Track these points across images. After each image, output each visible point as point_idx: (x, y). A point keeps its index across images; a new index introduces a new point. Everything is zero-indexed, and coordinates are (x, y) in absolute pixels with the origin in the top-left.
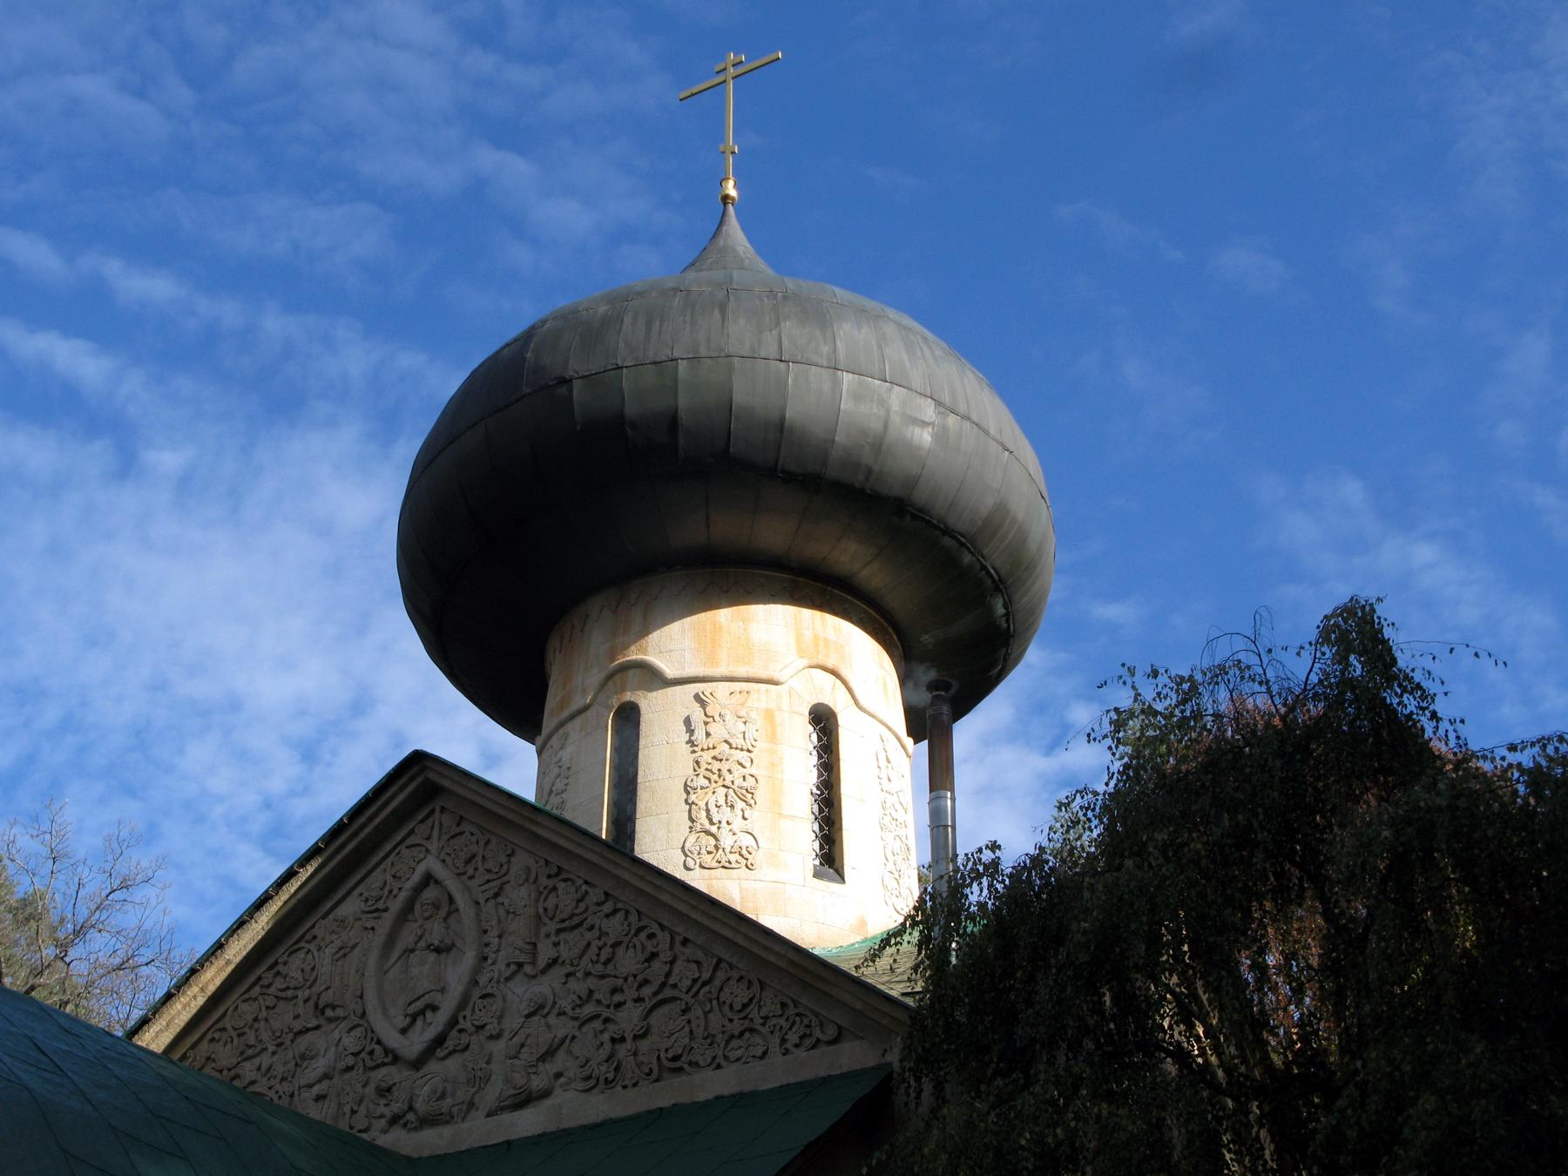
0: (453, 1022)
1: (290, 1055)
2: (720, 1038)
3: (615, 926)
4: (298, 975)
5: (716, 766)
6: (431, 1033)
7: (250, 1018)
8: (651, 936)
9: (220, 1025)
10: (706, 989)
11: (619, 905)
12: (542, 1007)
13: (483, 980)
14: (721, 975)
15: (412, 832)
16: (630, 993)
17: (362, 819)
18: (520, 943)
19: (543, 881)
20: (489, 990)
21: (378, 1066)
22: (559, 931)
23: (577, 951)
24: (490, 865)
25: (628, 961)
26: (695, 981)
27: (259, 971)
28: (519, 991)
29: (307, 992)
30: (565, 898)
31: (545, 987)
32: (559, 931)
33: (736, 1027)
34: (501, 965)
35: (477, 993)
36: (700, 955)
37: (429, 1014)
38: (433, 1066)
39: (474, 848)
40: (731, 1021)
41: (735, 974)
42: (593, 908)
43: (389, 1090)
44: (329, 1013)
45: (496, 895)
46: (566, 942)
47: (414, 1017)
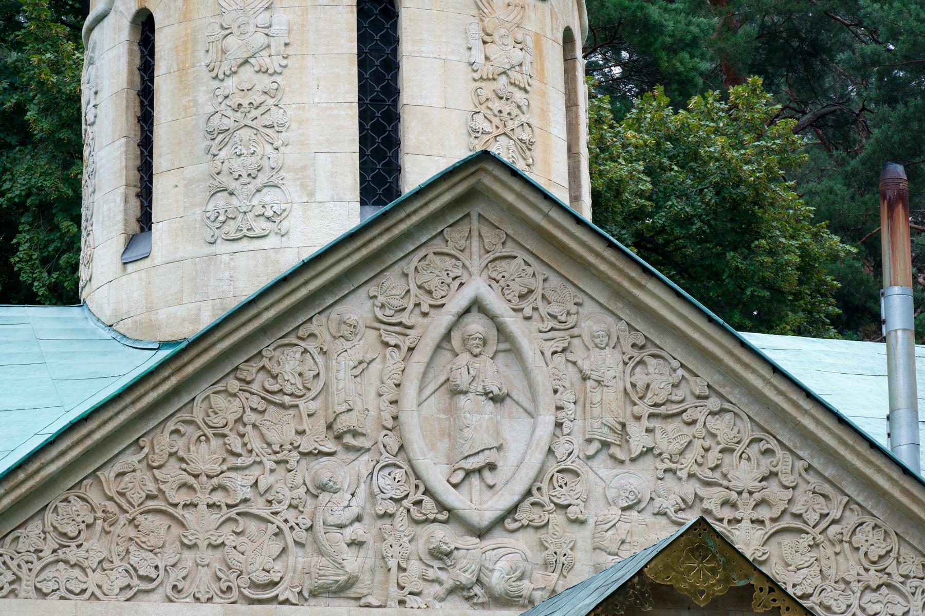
0: (529, 493)
1: (299, 480)
2: (854, 585)
3: (723, 427)
4: (298, 381)
5: (496, 105)
7: (232, 418)
8: (768, 452)
9: (186, 416)
10: (834, 529)
11: (727, 406)
12: (639, 502)
13: (561, 451)
14: (852, 519)
16: (745, 513)
17: (403, 214)
18: (611, 421)
19: (631, 352)
20: (568, 464)
21: (427, 521)
22: (651, 416)
23: (676, 447)
24: (555, 309)
25: (744, 474)
26: (823, 516)
27: (239, 360)
28: (603, 472)
29: (313, 406)
30: (658, 378)
31: (640, 479)
32: (651, 416)
33: (874, 578)
34: (578, 440)
35: (553, 468)
36: (827, 489)
37: (486, 474)
38: (498, 538)
39: (533, 283)
40: (867, 570)
41: (871, 522)
42: (691, 401)
43: (448, 554)
44: (348, 439)
45: (564, 350)
46: (664, 432)
47: (468, 473)
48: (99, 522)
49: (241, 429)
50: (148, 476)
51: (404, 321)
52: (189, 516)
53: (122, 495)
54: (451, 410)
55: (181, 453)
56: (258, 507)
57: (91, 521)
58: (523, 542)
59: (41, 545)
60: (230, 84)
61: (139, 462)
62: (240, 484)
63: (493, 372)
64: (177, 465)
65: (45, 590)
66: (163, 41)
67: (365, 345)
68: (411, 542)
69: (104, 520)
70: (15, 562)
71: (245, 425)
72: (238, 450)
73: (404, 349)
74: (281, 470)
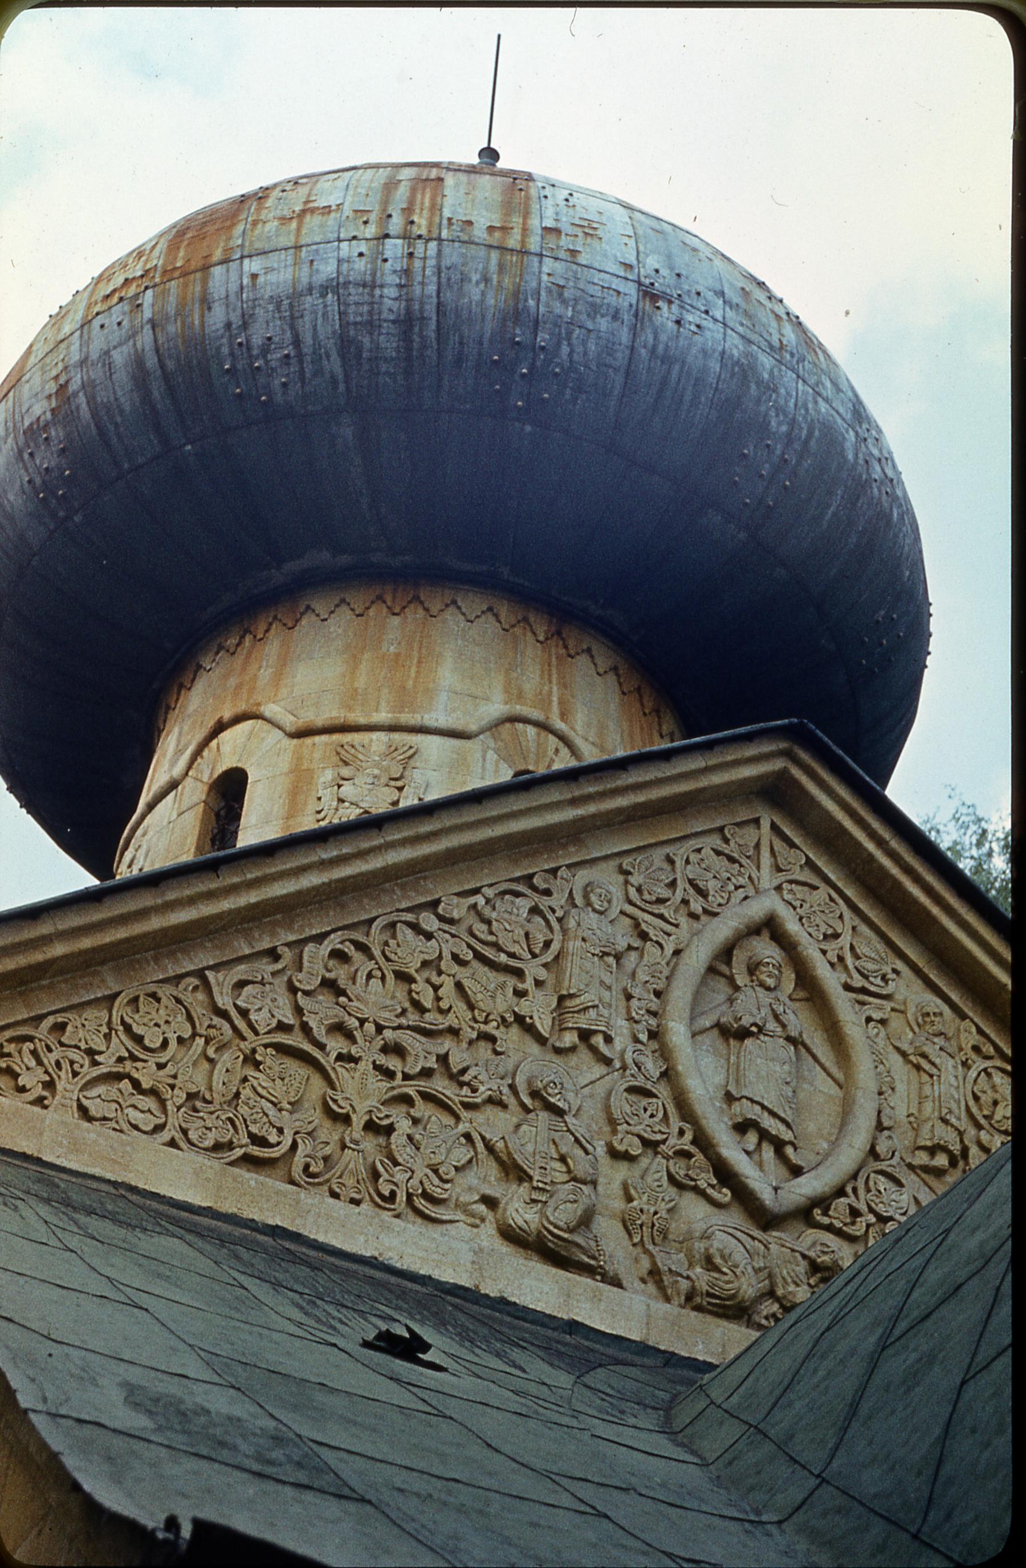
15: (721, 830)
48: (200, 1041)
49: (436, 980)
50: (284, 1000)
51: (667, 915)
52: (341, 1073)
53: (244, 1013)
55: (342, 983)
57: (186, 1035)
59: (98, 1044)
61: (274, 974)
64: (332, 999)
65: (93, 1112)
69: (208, 1041)
70: (53, 1057)
71: (440, 973)
72: (428, 1004)
73: (669, 950)
74: (484, 1050)
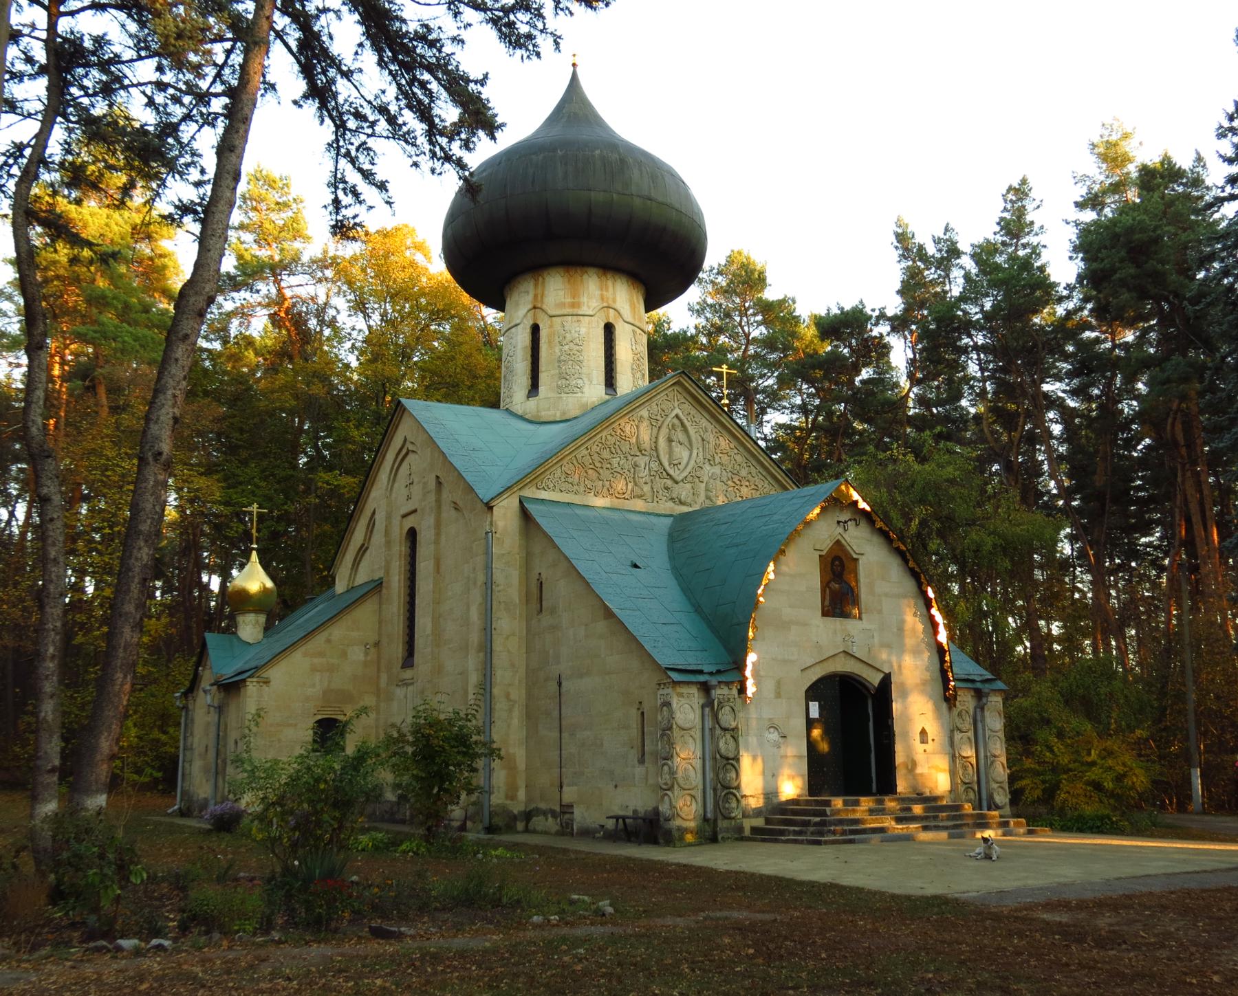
3: (738, 458)
6: (685, 474)
25: (744, 473)
30: (724, 443)
31: (717, 470)
54: (670, 447)
56: (619, 469)
58: (689, 486)
60: (566, 347)
62: (615, 462)
63: (681, 436)
66: (544, 333)
67: (645, 423)
68: (659, 484)
